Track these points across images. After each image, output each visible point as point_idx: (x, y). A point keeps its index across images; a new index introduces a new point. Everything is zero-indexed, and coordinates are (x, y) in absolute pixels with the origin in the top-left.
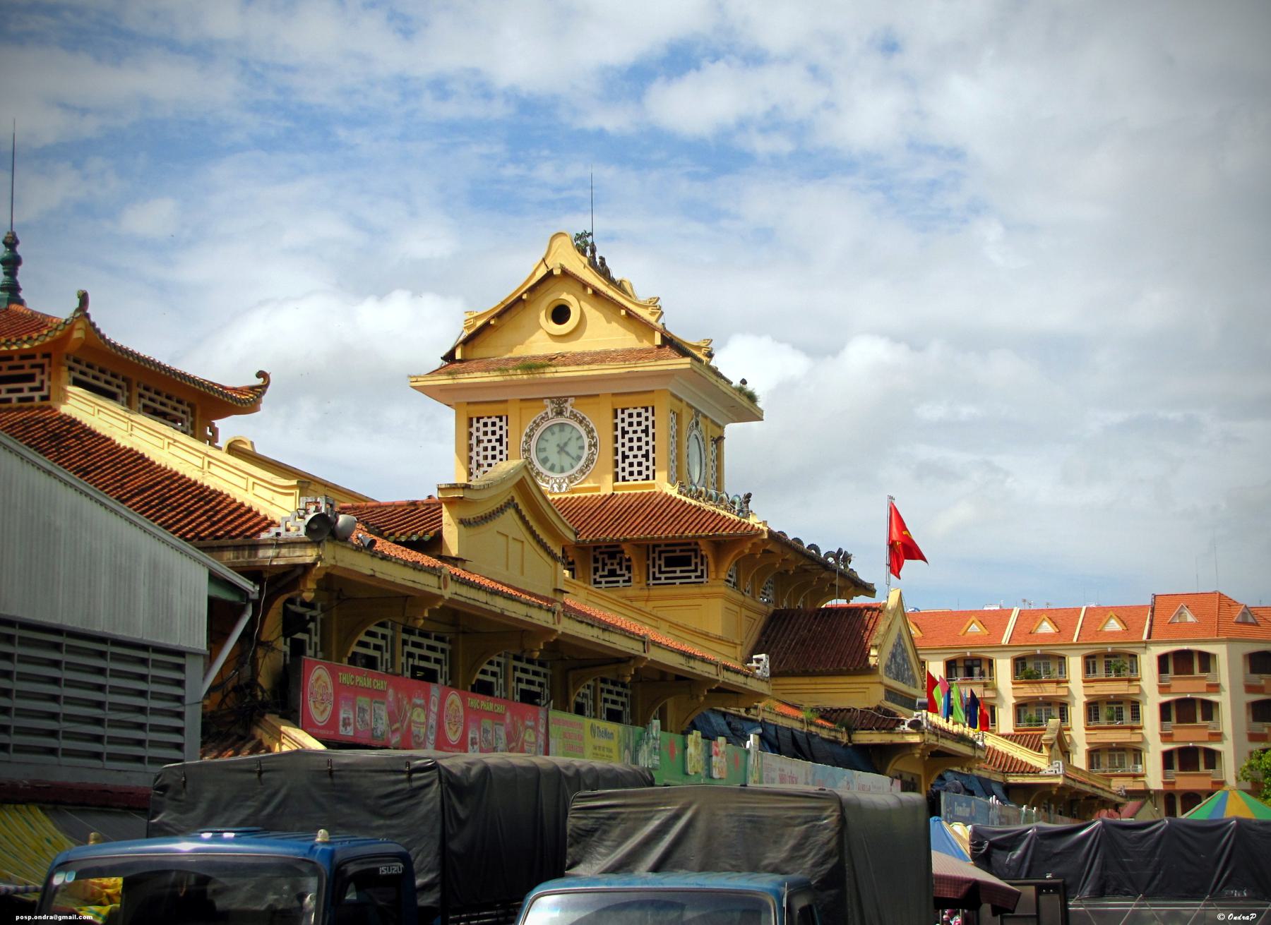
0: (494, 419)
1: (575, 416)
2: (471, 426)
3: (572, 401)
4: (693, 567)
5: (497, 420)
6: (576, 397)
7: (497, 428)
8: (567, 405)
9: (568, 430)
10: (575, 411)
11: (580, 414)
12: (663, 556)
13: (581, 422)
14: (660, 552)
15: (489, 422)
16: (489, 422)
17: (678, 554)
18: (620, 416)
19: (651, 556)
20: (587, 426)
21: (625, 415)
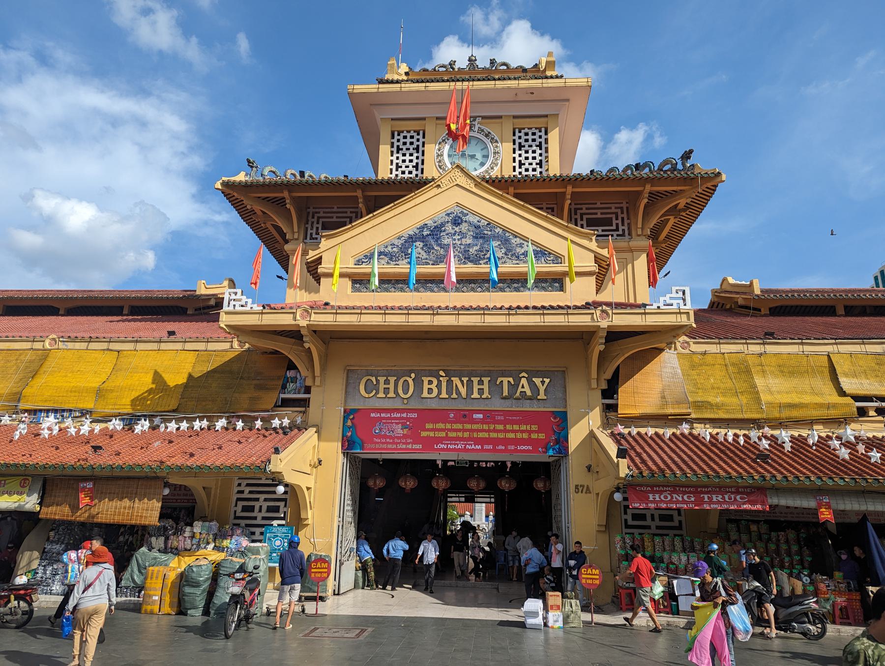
0: (412, 133)
1: (483, 131)
2: (393, 137)
3: (479, 120)
4: (614, 227)
5: (415, 134)
6: (483, 118)
7: (414, 140)
8: (476, 123)
9: (473, 142)
10: (483, 127)
11: (487, 129)
12: (585, 217)
13: (487, 136)
14: (582, 215)
15: (408, 135)
16: (408, 135)
17: (599, 216)
18: (517, 134)
19: (574, 217)
20: (492, 139)
21: (522, 134)
